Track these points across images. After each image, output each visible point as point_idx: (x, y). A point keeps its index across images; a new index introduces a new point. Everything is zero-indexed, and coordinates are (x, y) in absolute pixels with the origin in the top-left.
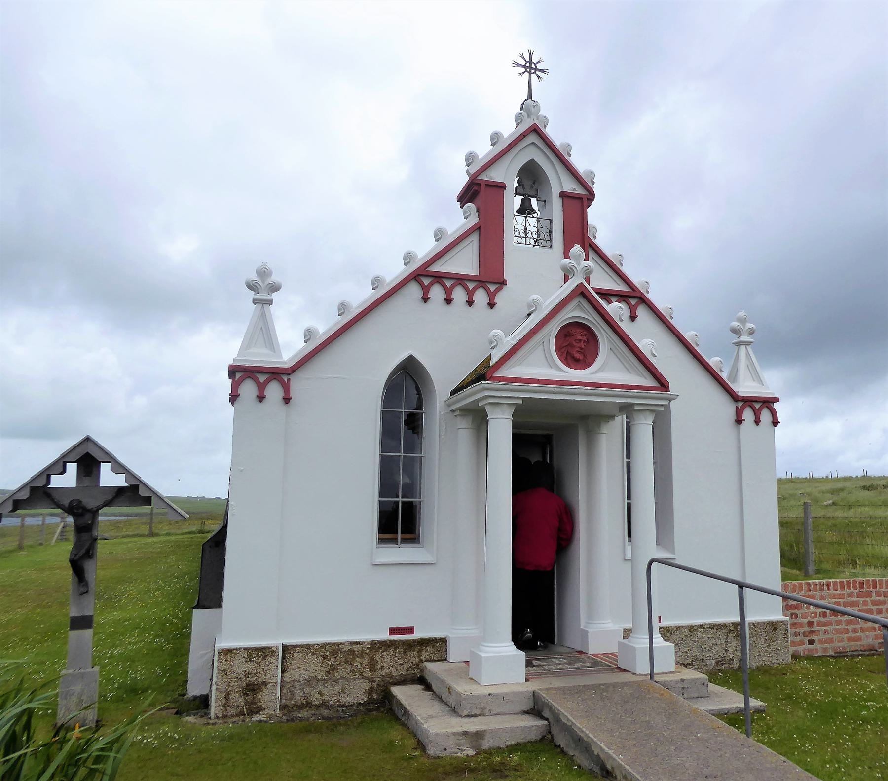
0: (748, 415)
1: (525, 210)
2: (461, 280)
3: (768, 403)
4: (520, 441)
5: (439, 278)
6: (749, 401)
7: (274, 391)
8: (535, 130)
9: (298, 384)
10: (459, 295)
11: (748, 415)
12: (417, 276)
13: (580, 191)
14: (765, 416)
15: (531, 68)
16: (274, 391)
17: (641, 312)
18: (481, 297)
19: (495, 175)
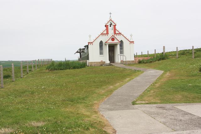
0: (131, 43)
1: (110, 26)
2: (105, 34)
3: (133, 42)
4: (109, 46)
5: (103, 34)
6: (131, 42)
7: (91, 44)
8: (111, 20)
9: (93, 43)
10: (105, 35)
11: (131, 43)
12: (101, 34)
13: (115, 25)
14: (133, 43)
15: (110, 14)
16: (91, 44)
17: (121, 35)
18: (107, 35)
19: (107, 25)
